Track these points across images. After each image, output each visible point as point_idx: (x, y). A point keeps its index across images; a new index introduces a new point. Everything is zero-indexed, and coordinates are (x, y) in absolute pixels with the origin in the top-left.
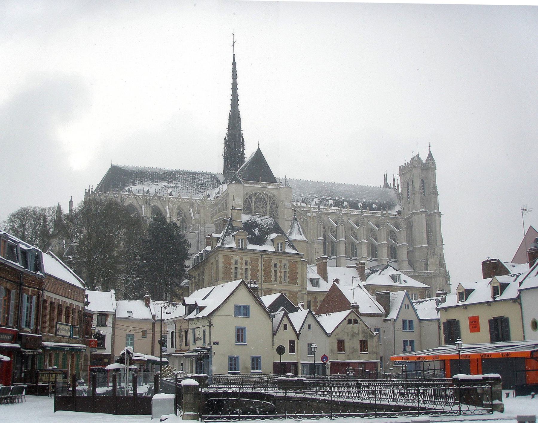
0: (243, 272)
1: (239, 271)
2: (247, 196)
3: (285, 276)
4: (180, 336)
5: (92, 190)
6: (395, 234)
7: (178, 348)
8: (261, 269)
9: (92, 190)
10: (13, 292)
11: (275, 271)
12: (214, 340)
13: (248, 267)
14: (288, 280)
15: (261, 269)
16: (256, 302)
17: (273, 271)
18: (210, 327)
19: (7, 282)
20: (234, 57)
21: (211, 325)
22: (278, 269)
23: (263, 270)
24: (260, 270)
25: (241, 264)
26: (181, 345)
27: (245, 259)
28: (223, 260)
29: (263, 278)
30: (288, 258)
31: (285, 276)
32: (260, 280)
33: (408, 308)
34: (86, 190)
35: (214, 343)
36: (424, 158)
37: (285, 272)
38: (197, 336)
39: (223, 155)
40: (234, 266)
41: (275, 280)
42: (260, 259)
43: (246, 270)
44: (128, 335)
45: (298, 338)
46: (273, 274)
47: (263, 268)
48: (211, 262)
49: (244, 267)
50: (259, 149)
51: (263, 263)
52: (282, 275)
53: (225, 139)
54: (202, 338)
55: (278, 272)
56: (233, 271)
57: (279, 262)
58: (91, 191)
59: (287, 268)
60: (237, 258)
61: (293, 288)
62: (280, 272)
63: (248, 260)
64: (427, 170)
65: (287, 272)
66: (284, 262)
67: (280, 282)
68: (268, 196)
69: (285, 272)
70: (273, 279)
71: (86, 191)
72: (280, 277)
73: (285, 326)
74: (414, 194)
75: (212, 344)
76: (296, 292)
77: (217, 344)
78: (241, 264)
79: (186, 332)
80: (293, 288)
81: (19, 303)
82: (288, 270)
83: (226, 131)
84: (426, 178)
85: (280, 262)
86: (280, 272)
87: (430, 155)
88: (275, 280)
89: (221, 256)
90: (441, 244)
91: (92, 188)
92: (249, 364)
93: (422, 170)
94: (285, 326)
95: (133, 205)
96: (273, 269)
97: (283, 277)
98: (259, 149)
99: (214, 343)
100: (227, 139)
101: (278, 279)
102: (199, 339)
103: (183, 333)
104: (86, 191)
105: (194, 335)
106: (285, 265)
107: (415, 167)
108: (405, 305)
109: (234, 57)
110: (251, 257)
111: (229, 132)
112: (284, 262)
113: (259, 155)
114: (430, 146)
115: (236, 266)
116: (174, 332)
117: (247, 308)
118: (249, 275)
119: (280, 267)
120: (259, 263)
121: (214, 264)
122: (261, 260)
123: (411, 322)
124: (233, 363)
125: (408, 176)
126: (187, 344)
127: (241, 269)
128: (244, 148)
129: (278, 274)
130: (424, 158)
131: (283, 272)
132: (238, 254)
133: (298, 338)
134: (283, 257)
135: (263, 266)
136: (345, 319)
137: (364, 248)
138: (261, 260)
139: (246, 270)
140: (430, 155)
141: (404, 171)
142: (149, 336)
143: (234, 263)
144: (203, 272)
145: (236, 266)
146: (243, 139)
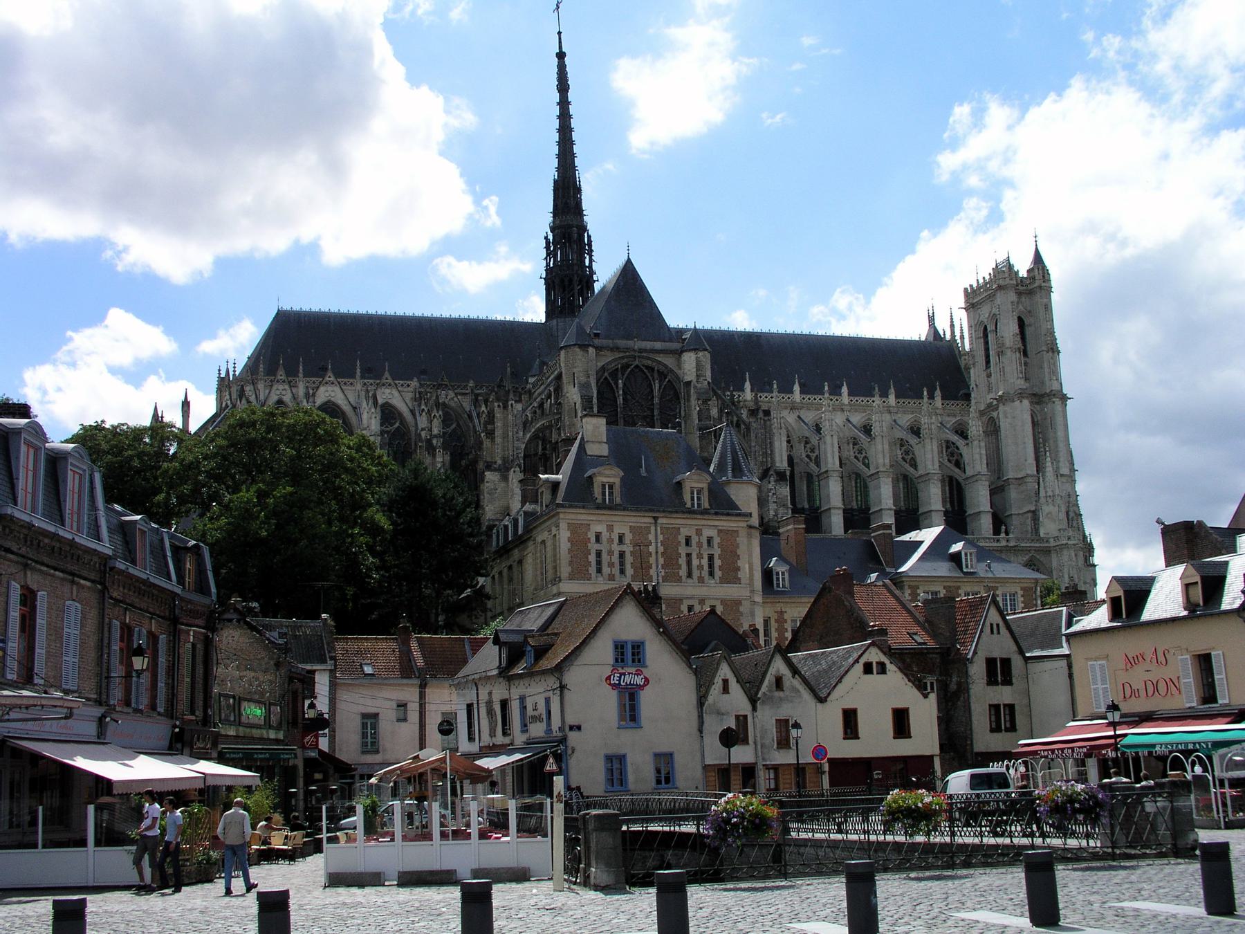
0: (616, 558)
1: (605, 557)
2: (606, 374)
3: (711, 566)
4: (490, 712)
5: (234, 371)
6: (958, 448)
7: (486, 740)
8: (657, 552)
9: (234, 371)
10: (163, 638)
11: (689, 555)
12: (571, 720)
13: (628, 549)
14: (718, 573)
15: (657, 552)
16: (659, 632)
17: (683, 555)
18: (562, 692)
19: (151, 618)
20: (560, 39)
21: (562, 687)
23: (660, 553)
24: (654, 555)
25: (611, 541)
26: (492, 734)
28: (568, 534)
30: (717, 523)
31: (711, 566)
33: (999, 633)
34: (219, 370)
35: (571, 728)
36: (1023, 266)
37: (711, 558)
38: (530, 712)
39: (544, 276)
40: (593, 547)
41: (690, 575)
42: (653, 529)
43: (622, 555)
44: (365, 716)
45: (754, 709)
46: (683, 561)
47: (661, 549)
48: (539, 539)
49: (616, 548)
50: (629, 259)
51: (661, 538)
52: (705, 562)
53: (546, 238)
54: (544, 717)
55: (694, 556)
56: (592, 558)
58: (231, 374)
59: (716, 546)
60: (601, 528)
61: (731, 591)
62: (700, 556)
63: (626, 531)
64: (1030, 293)
65: (716, 557)
66: (707, 533)
67: (701, 580)
68: (656, 371)
69: (711, 558)
70: (683, 572)
71: (220, 374)
72: (700, 567)
73: (726, 682)
74: (1000, 354)
75: (567, 729)
76: (738, 602)
77: (579, 728)
79: (504, 704)
80: (731, 591)
81: (174, 661)
82: (717, 552)
83: (550, 218)
84: (1030, 312)
86: (700, 556)
87: (1038, 259)
88: (690, 575)
89: (563, 525)
90: (1070, 470)
91: (235, 367)
92: (649, 773)
93: (1019, 294)
94: (726, 682)
95: (334, 404)
96: (683, 550)
97: (706, 567)
98: (629, 259)
99: (571, 728)
100: (551, 237)
101: (696, 573)
102: (536, 719)
103: (497, 708)
104: (220, 374)
105: (523, 708)
106: (710, 540)
107: (1000, 288)
108: (992, 625)
109: (560, 39)
110: (631, 524)
111: (554, 222)
113: (629, 277)
115: (597, 547)
116: (475, 706)
117: (638, 648)
119: (700, 545)
120: (651, 537)
121: (549, 543)
122: (656, 530)
123: (1006, 662)
124: (616, 765)
125: (985, 312)
127: (611, 553)
128: (591, 257)
129: (695, 562)
130: (1023, 266)
131: (706, 557)
132: (603, 518)
133: (754, 709)
134: (703, 522)
135: (659, 544)
137: (886, 486)
138: (656, 530)
139: (622, 555)
140: (1038, 259)
141: (975, 299)
142: (414, 716)
143: (593, 539)
144: (520, 562)
145: (597, 547)
146: (589, 237)
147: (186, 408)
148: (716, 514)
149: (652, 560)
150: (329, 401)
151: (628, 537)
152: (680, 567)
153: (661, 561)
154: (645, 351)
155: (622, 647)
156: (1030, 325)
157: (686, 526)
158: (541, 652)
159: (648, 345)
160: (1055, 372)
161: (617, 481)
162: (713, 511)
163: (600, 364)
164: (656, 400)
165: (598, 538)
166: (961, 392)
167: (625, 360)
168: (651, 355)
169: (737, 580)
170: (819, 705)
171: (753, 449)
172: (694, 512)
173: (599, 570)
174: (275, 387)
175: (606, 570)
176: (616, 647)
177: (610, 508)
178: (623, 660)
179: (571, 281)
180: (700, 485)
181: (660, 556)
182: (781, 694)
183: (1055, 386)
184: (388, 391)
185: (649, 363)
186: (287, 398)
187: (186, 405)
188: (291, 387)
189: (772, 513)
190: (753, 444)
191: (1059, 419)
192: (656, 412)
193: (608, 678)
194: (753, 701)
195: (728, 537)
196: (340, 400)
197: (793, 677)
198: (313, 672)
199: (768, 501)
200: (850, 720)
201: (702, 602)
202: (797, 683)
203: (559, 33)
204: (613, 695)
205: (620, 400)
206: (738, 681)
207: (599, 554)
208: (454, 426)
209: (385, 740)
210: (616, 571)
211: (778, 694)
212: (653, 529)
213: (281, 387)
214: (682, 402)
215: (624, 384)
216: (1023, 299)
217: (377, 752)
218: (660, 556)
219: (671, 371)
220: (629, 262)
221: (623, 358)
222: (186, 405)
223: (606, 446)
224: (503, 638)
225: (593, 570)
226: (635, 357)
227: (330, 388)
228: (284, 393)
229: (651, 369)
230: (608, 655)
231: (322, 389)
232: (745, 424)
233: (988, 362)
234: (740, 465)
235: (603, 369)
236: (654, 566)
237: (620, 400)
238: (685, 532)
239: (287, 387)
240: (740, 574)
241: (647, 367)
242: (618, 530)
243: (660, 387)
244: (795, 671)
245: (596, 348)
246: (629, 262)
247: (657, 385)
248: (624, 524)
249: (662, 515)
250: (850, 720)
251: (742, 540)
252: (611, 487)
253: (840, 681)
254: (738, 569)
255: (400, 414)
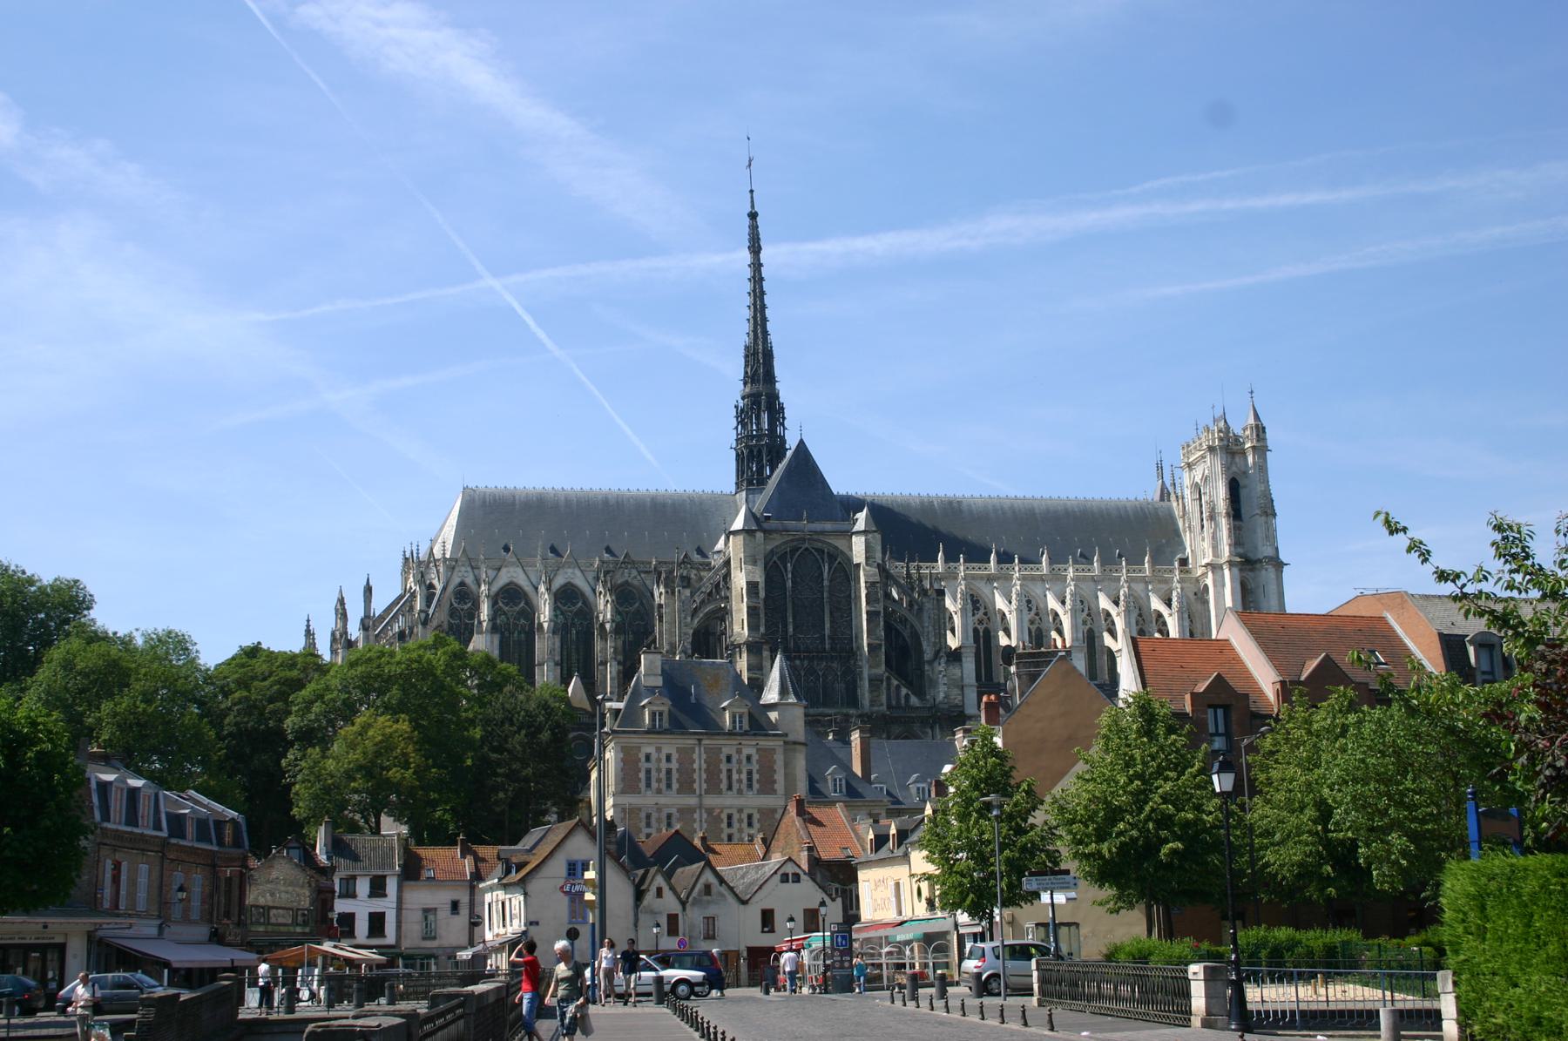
0: (663, 775)
1: (654, 774)
2: (775, 558)
3: (750, 780)
5: (418, 554)
8: (700, 769)
9: (418, 554)
11: (729, 771)
13: (674, 765)
14: (756, 786)
22: (734, 766)
24: (697, 771)
25: (659, 760)
27: (666, 750)
29: (704, 786)
31: (750, 780)
32: (698, 792)
35: (531, 923)
37: (750, 773)
40: (643, 765)
41: (730, 788)
43: (669, 772)
45: (684, 909)
46: (724, 776)
47: (704, 766)
49: (664, 765)
51: (704, 756)
52: (744, 776)
55: (734, 772)
56: (642, 775)
57: (737, 752)
60: (650, 750)
62: (739, 772)
65: (754, 771)
66: (746, 751)
68: (826, 555)
69: (750, 773)
70: (724, 786)
72: (740, 781)
77: (537, 923)
78: (659, 760)
82: (755, 767)
85: (739, 752)
86: (739, 772)
88: (730, 788)
95: (516, 585)
96: (724, 767)
97: (745, 781)
99: (531, 923)
101: (735, 786)
106: (749, 758)
112: (746, 751)
114: (1252, 392)
118: (674, 781)
119: (739, 761)
120: (695, 756)
126: (504, 926)
127: (659, 770)
129: (735, 776)
133: (684, 909)
136: (776, 872)
139: (669, 772)
143: (643, 759)
147: (368, 594)
148: (755, 735)
149: (696, 776)
150: (511, 583)
151: (675, 757)
152: (721, 781)
153: (704, 776)
154: (816, 532)
155: (574, 865)
156: (1245, 487)
157: (728, 746)
158: (520, 867)
159: (818, 526)
160: (1271, 537)
161: (665, 709)
162: (753, 732)
163: (769, 548)
164: (826, 583)
165: (648, 758)
166: (1178, 556)
167: (795, 543)
168: (821, 537)
169: (774, 792)
170: (742, 907)
171: (926, 630)
172: (735, 734)
173: (648, 785)
174: (457, 569)
175: (654, 785)
176: (570, 864)
177: (659, 733)
178: (574, 875)
179: (760, 452)
180: (742, 710)
181: (703, 772)
182: (709, 898)
183: (1267, 551)
184: (570, 571)
185: (819, 545)
186: (469, 580)
187: (368, 590)
188: (473, 568)
189: (942, 695)
190: (926, 624)
191: (1272, 588)
192: (825, 595)
193: (562, 887)
194: (683, 904)
195: (766, 757)
196: (522, 580)
197: (721, 885)
198: (384, 877)
199: (937, 682)
200: (767, 918)
201: (740, 811)
202: (723, 889)
203: (752, 191)
204: (566, 900)
205: (789, 584)
206: (670, 889)
207: (648, 771)
208: (637, 605)
209: (442, 931)
210: (663, 786)
211: (705, 898)
212: (697, 749)
213: (463, 569)
214: (853, 583)
215: (794, 568)
216: (1237, 459)
217: (435, 938)
218: (703, 772)
219: (842, 552)
220: (801, 442)
221: (792, 541)
222: (368, 590)
223: (661, 678)
224: (502, 856)
225: (642, 785)
226: (804, 540)
227: (512, 569)
228: (466, 574)
229: (821, 551)
230: (563, 871)
231: (504, 570)
232: (917, 604)
233: (1202, 527)
234: (787, 689)
235: (772, 551)
236: (697, 781)
237: (789, 584)
238: (726, 751)
239: (469, 569)
240: (776, 786)
241: (816, 550)
242: (666, 750)
243: (830, 569)
244: (722, 881)
245: (765, 531)
246: (801, 442)
247: (827, 567)
248: (670, 745)
249: (705, 737)
250: (767, 918)
251: (779, 758)
252: (661, 714)
253: (760, 888)
254: (775, 782)
255: (583, 595)
